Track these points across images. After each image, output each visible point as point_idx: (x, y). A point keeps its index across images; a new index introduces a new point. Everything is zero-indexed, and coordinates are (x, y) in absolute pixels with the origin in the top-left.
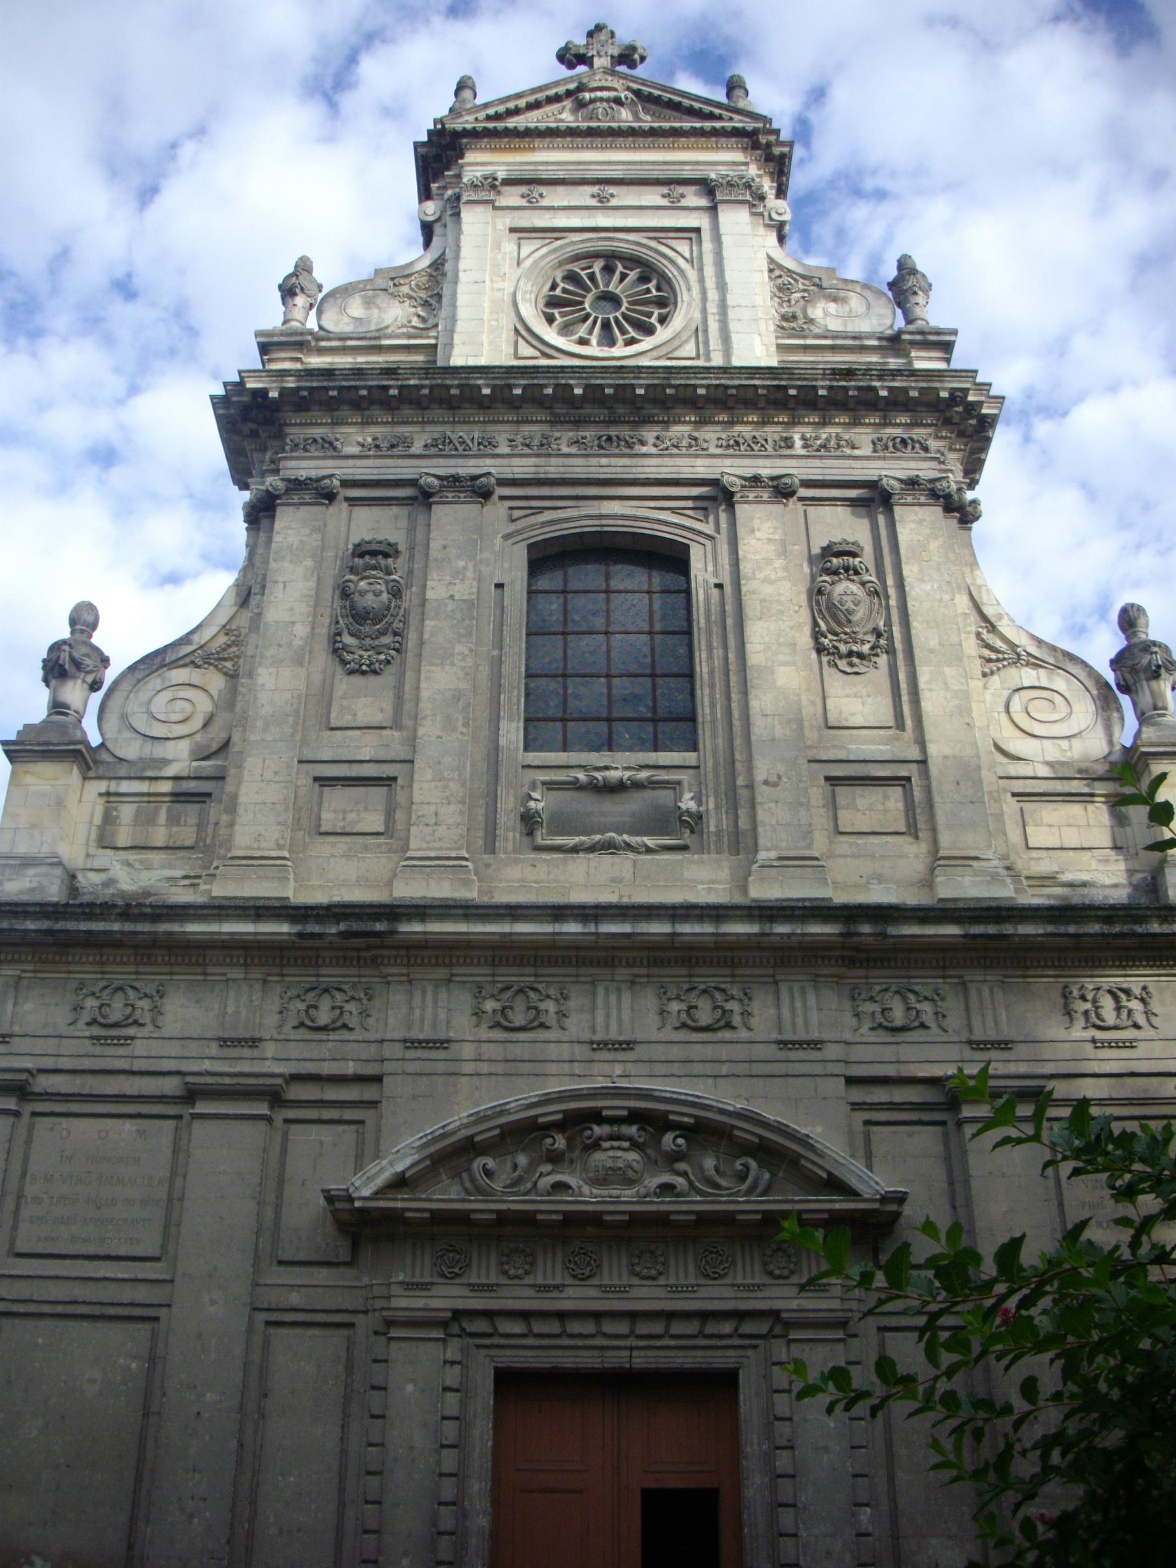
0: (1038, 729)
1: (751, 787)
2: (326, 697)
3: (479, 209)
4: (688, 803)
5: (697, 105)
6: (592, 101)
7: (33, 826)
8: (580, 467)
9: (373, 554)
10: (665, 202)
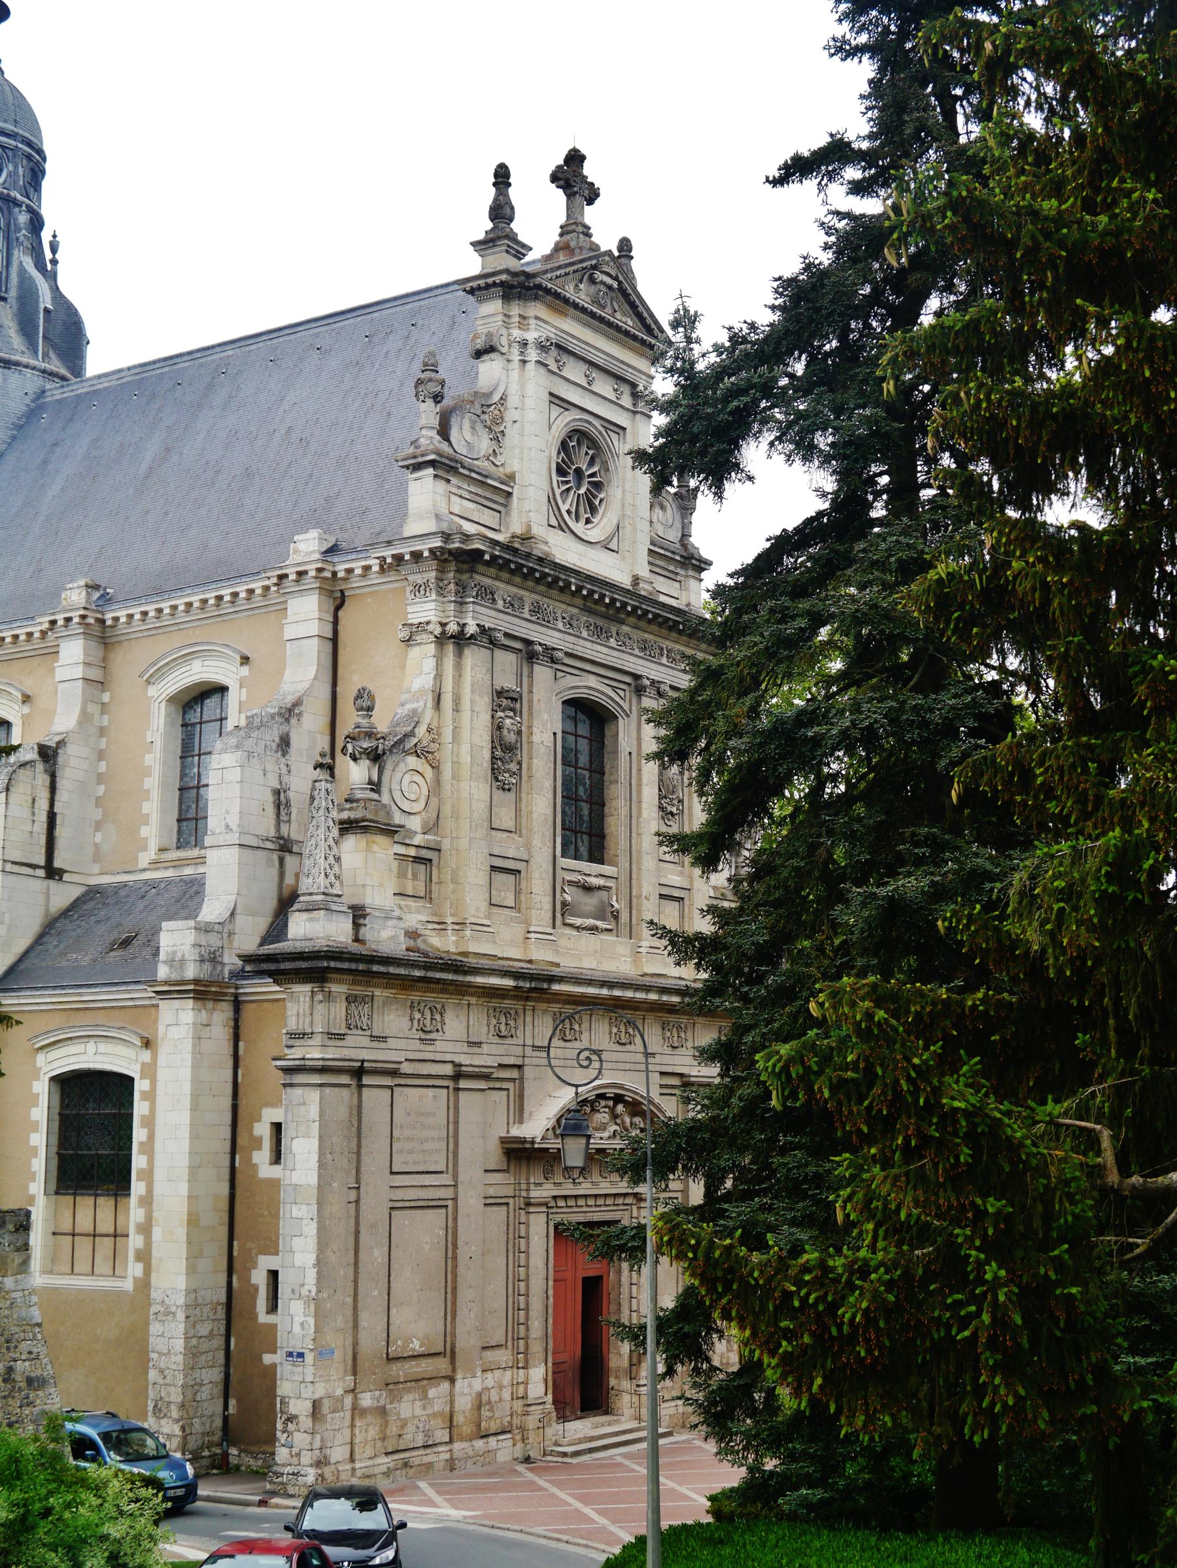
1: (639, 896)
5: (645, 315)
6: (602, 283)
7: (381, 885)
10: (611, 396)
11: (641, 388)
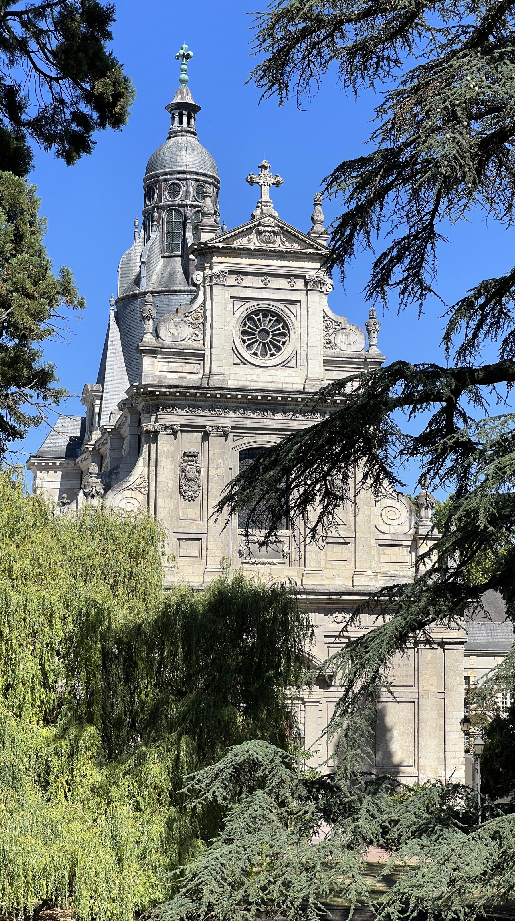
0: (389, 522)
2: (178, 509)
3: (220, 287)
4: (287, 550)
6: (264, 231)
8: (257, 423)
9: (191, 456)
11: (307, 277)
